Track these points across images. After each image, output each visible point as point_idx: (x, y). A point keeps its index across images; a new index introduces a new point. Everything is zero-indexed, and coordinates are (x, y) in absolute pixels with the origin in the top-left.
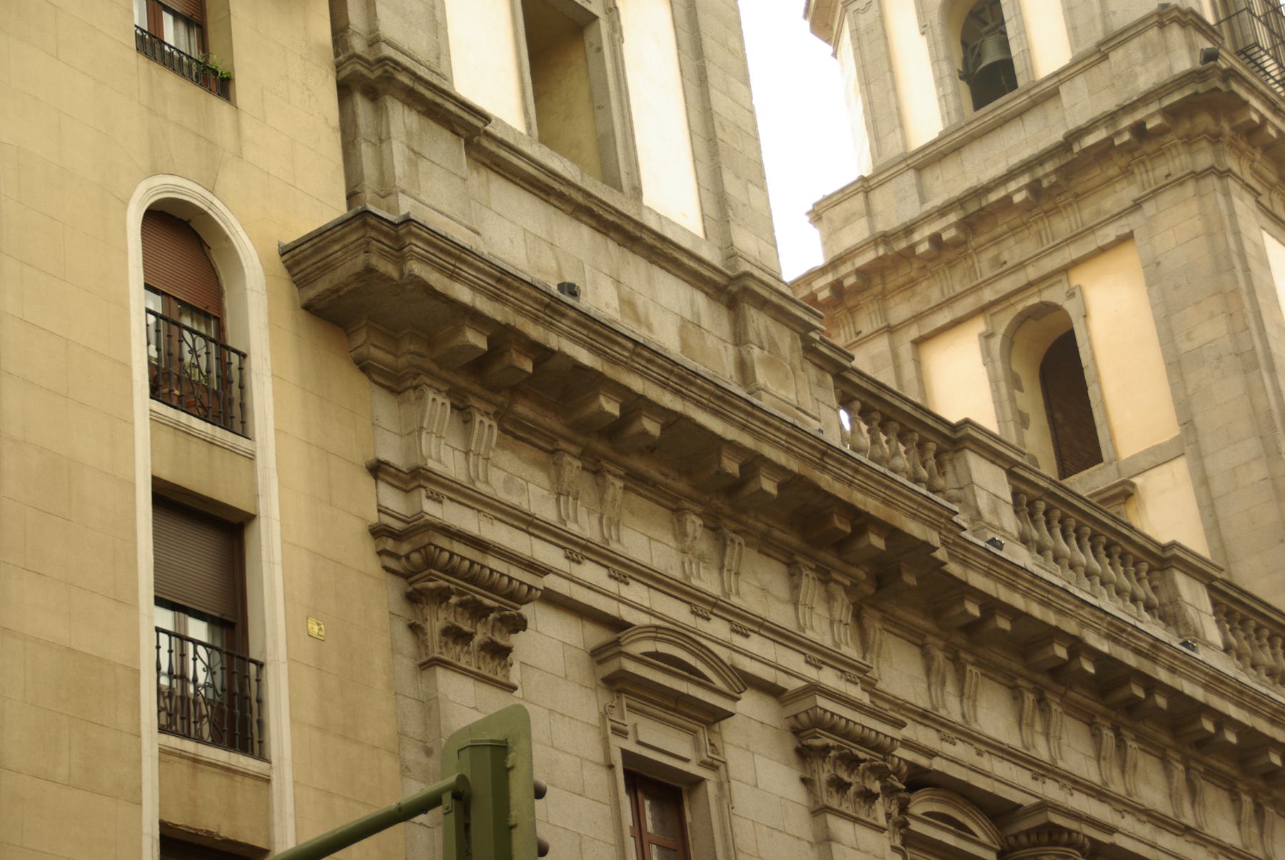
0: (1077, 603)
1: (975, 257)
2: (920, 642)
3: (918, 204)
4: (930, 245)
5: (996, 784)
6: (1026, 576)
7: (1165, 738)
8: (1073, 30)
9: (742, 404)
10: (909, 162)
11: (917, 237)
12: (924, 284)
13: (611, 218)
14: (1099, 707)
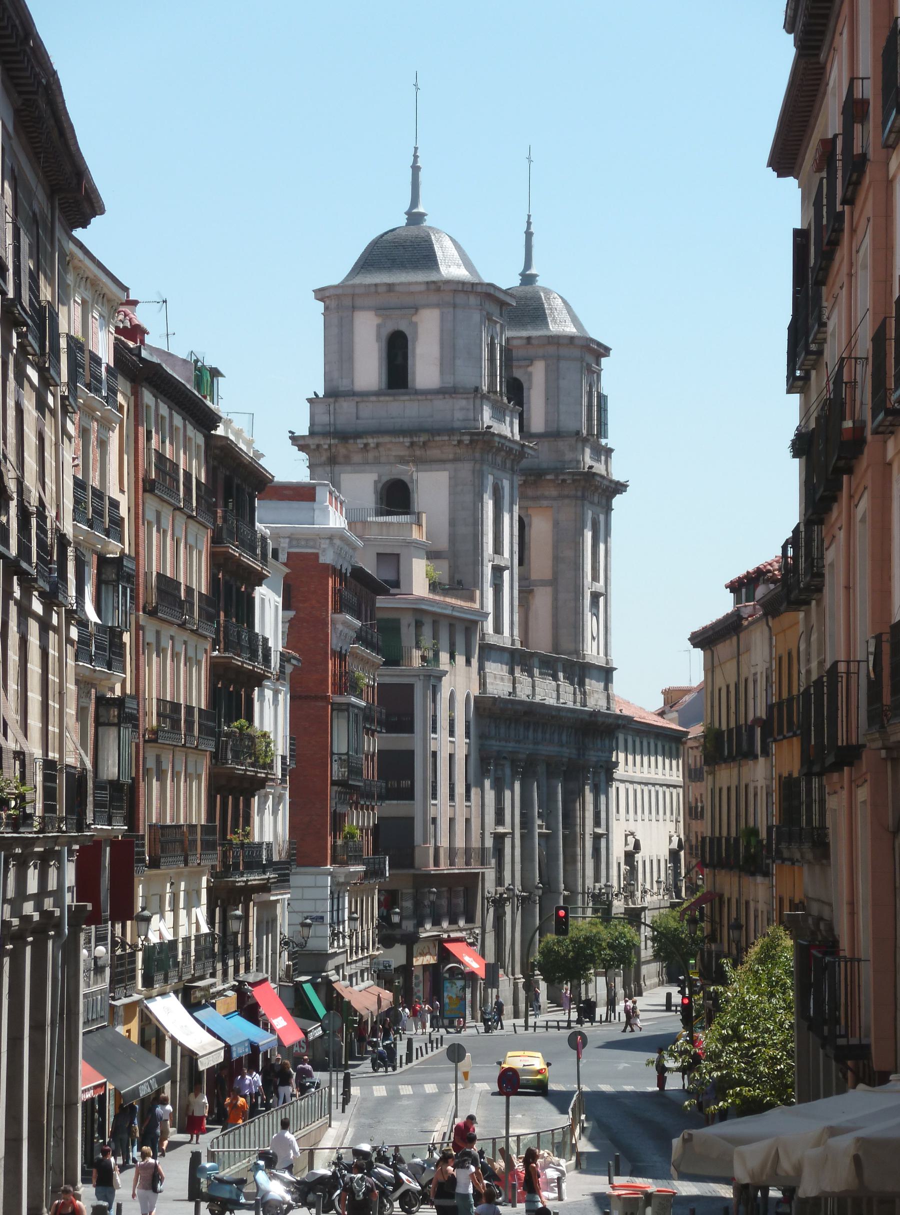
8: (546, 421)
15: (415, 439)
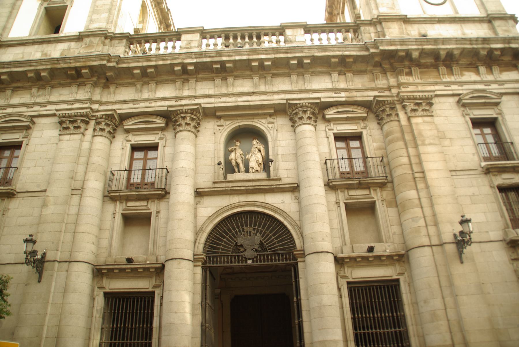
0: (178, 55)
2: (135, 85)
5: (157, 108)
6: (153, 56)
7: (248, 73)
9: (27, 62)
13: (40, 41)
14: (213, 75)
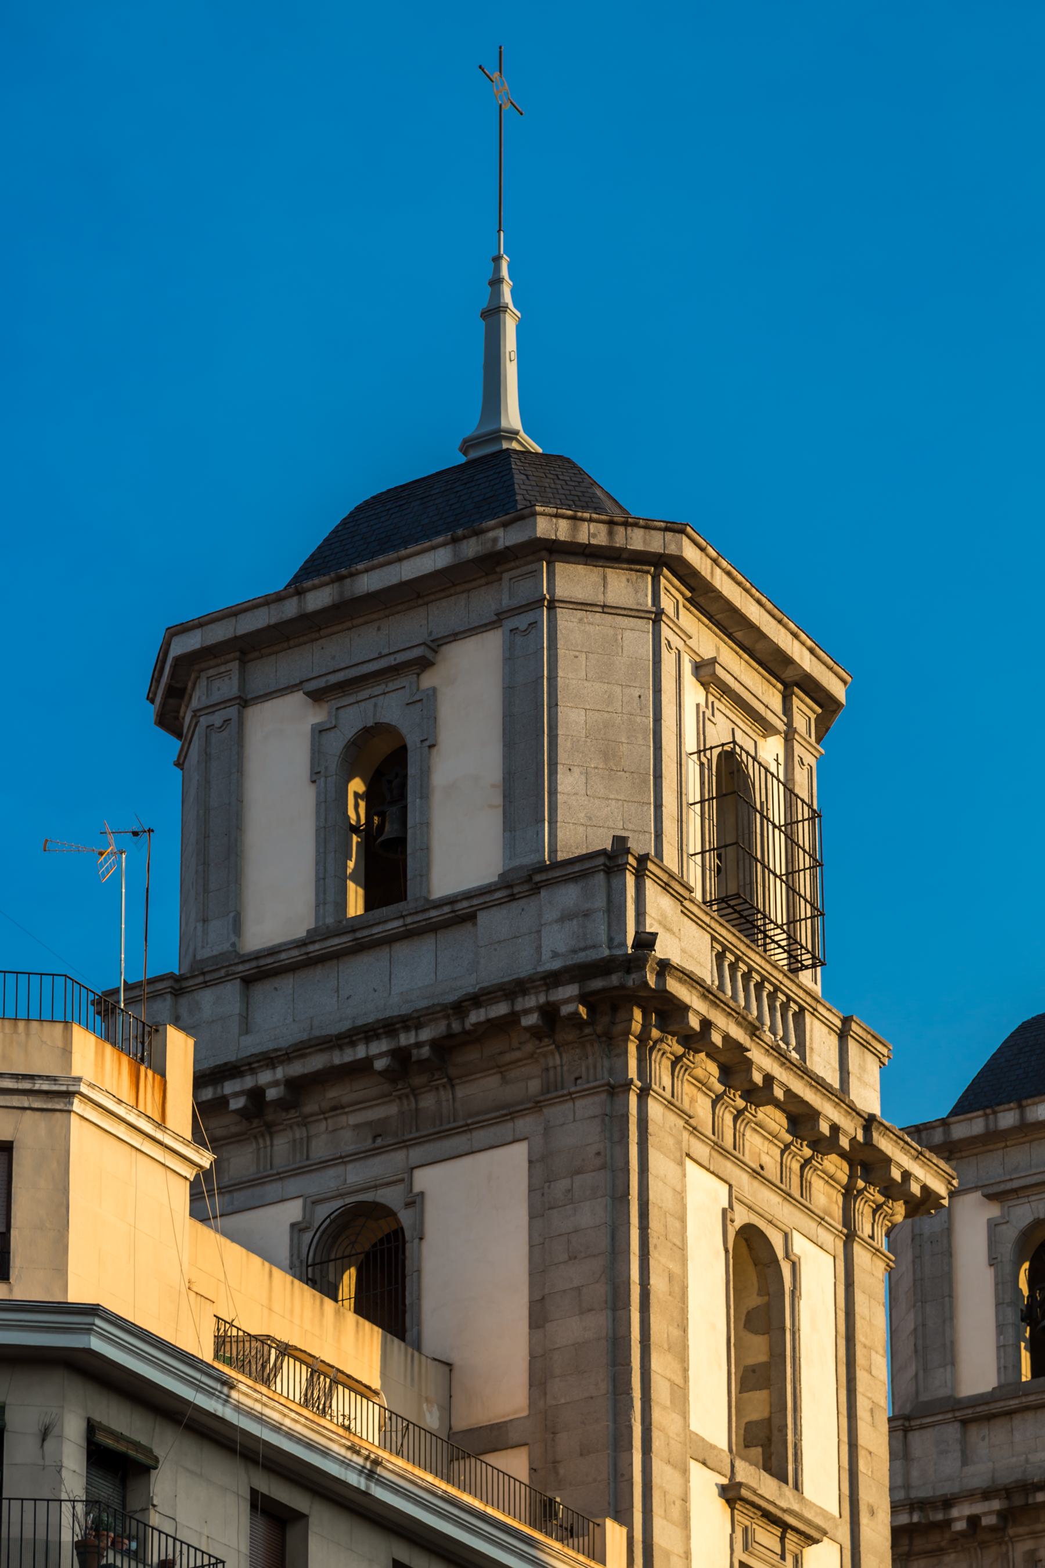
1: (1010, 1545)
3: (959, 1464)
4: (967, 1524)
10: (958, 1414)
11: (955, 1513)
12: (953, 1556)
15: (405, 1039)
